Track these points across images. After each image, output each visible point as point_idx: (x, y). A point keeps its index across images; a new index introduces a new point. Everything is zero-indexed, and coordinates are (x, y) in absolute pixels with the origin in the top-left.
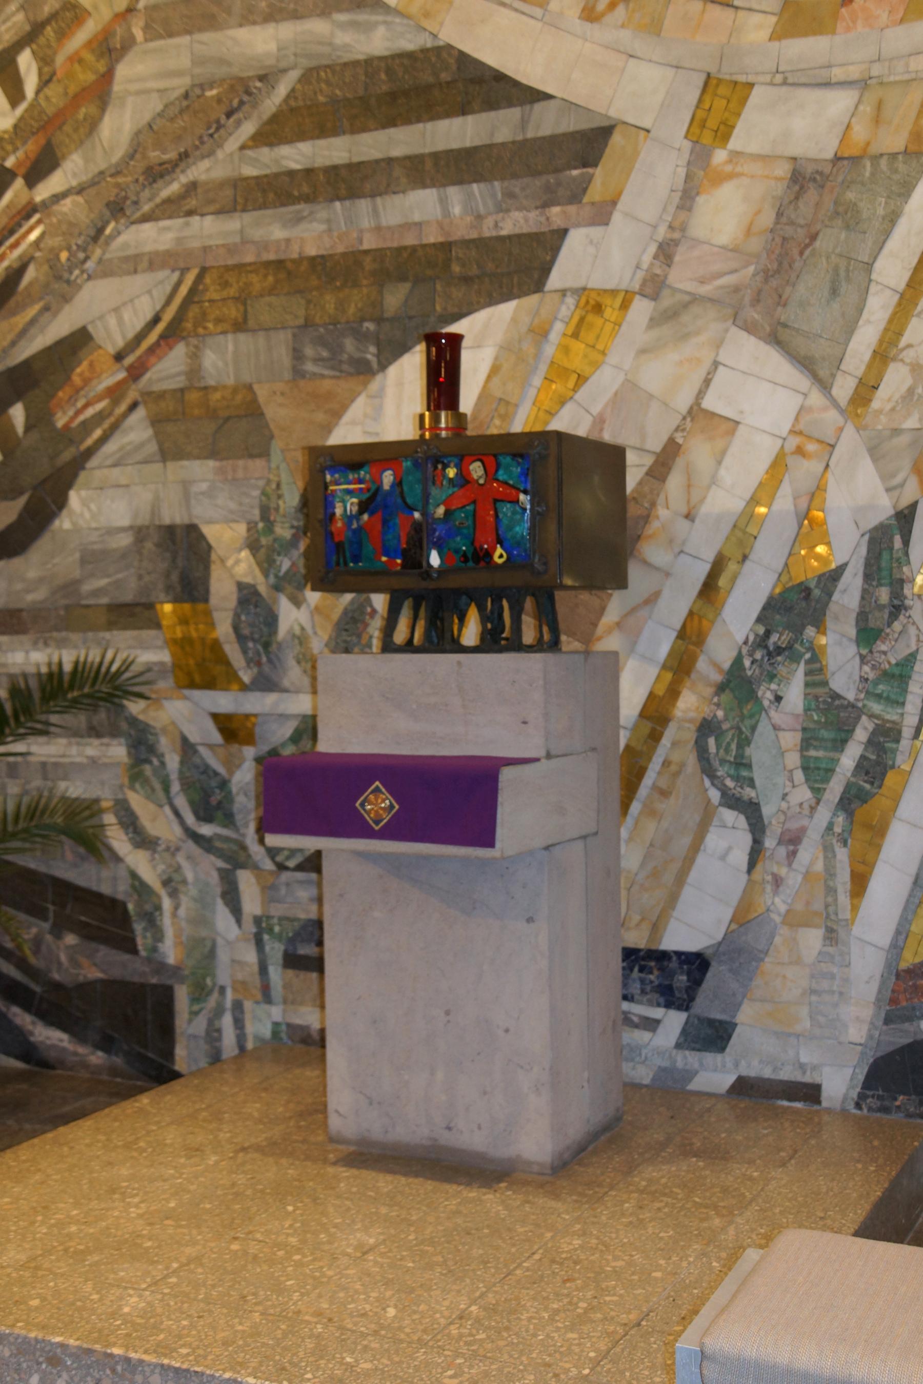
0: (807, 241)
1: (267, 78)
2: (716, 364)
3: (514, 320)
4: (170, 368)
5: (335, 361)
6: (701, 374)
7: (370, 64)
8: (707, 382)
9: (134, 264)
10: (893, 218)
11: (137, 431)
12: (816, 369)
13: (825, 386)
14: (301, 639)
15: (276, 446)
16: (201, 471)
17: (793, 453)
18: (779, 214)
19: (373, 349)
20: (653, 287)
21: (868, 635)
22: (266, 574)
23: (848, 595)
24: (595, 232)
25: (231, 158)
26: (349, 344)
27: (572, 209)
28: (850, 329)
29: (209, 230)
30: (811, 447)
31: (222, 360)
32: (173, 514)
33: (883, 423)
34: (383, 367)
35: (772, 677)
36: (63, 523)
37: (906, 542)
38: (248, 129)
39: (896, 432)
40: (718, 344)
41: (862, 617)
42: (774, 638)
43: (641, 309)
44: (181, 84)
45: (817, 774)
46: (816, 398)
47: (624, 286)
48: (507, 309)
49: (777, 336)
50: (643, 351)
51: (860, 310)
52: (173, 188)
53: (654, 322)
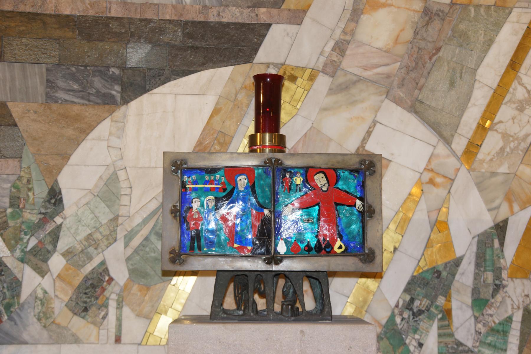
0: (434, 51)
2: (375, 123)
3: (231, 79)
5: (85, 94)
6: (365, 127)
8: (369, 133)
10: (489, 43)
12: (443, 132)
13: (448, 142)
14: (44, 301)
15: (28, 153)
17: (427, 183)
18: (416, 33)
19: (117, 88)
20: (332, 68)
21: (480, 303)
22: (12, 248)
23: (466, 276)
24: (292, 29)
26: (98, 83)
27: (274, 11)
28: (463, 108)
30: (439, 180)
33: (485, 168)
34: (126, 101)
35: (416, 331)
37: (502, 244)
39: (494, 174)
40: (377, 110)
41: (475, 291)
42: (417, 303)
43: (323, 82)
46: (442, 149)
47: (312, 65)
48: (226, 71)
49: (416, 108)
50: (325, 109)
51: (469, 96)
53: (332, 91)
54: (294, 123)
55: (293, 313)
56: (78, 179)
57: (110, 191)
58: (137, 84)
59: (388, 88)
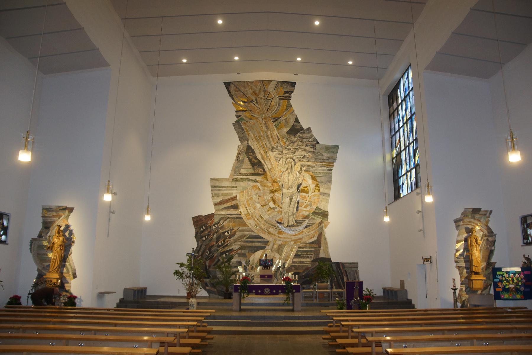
4: (239, 251)
11: (237, 255)
16: (242, 258)
25: (244, 239)
29: (243, 243)
31: (243, 251)
32: (239, 261)
56: (251, 259)
57: (253, 260)
58: (256, 251)
59: (276, 251)
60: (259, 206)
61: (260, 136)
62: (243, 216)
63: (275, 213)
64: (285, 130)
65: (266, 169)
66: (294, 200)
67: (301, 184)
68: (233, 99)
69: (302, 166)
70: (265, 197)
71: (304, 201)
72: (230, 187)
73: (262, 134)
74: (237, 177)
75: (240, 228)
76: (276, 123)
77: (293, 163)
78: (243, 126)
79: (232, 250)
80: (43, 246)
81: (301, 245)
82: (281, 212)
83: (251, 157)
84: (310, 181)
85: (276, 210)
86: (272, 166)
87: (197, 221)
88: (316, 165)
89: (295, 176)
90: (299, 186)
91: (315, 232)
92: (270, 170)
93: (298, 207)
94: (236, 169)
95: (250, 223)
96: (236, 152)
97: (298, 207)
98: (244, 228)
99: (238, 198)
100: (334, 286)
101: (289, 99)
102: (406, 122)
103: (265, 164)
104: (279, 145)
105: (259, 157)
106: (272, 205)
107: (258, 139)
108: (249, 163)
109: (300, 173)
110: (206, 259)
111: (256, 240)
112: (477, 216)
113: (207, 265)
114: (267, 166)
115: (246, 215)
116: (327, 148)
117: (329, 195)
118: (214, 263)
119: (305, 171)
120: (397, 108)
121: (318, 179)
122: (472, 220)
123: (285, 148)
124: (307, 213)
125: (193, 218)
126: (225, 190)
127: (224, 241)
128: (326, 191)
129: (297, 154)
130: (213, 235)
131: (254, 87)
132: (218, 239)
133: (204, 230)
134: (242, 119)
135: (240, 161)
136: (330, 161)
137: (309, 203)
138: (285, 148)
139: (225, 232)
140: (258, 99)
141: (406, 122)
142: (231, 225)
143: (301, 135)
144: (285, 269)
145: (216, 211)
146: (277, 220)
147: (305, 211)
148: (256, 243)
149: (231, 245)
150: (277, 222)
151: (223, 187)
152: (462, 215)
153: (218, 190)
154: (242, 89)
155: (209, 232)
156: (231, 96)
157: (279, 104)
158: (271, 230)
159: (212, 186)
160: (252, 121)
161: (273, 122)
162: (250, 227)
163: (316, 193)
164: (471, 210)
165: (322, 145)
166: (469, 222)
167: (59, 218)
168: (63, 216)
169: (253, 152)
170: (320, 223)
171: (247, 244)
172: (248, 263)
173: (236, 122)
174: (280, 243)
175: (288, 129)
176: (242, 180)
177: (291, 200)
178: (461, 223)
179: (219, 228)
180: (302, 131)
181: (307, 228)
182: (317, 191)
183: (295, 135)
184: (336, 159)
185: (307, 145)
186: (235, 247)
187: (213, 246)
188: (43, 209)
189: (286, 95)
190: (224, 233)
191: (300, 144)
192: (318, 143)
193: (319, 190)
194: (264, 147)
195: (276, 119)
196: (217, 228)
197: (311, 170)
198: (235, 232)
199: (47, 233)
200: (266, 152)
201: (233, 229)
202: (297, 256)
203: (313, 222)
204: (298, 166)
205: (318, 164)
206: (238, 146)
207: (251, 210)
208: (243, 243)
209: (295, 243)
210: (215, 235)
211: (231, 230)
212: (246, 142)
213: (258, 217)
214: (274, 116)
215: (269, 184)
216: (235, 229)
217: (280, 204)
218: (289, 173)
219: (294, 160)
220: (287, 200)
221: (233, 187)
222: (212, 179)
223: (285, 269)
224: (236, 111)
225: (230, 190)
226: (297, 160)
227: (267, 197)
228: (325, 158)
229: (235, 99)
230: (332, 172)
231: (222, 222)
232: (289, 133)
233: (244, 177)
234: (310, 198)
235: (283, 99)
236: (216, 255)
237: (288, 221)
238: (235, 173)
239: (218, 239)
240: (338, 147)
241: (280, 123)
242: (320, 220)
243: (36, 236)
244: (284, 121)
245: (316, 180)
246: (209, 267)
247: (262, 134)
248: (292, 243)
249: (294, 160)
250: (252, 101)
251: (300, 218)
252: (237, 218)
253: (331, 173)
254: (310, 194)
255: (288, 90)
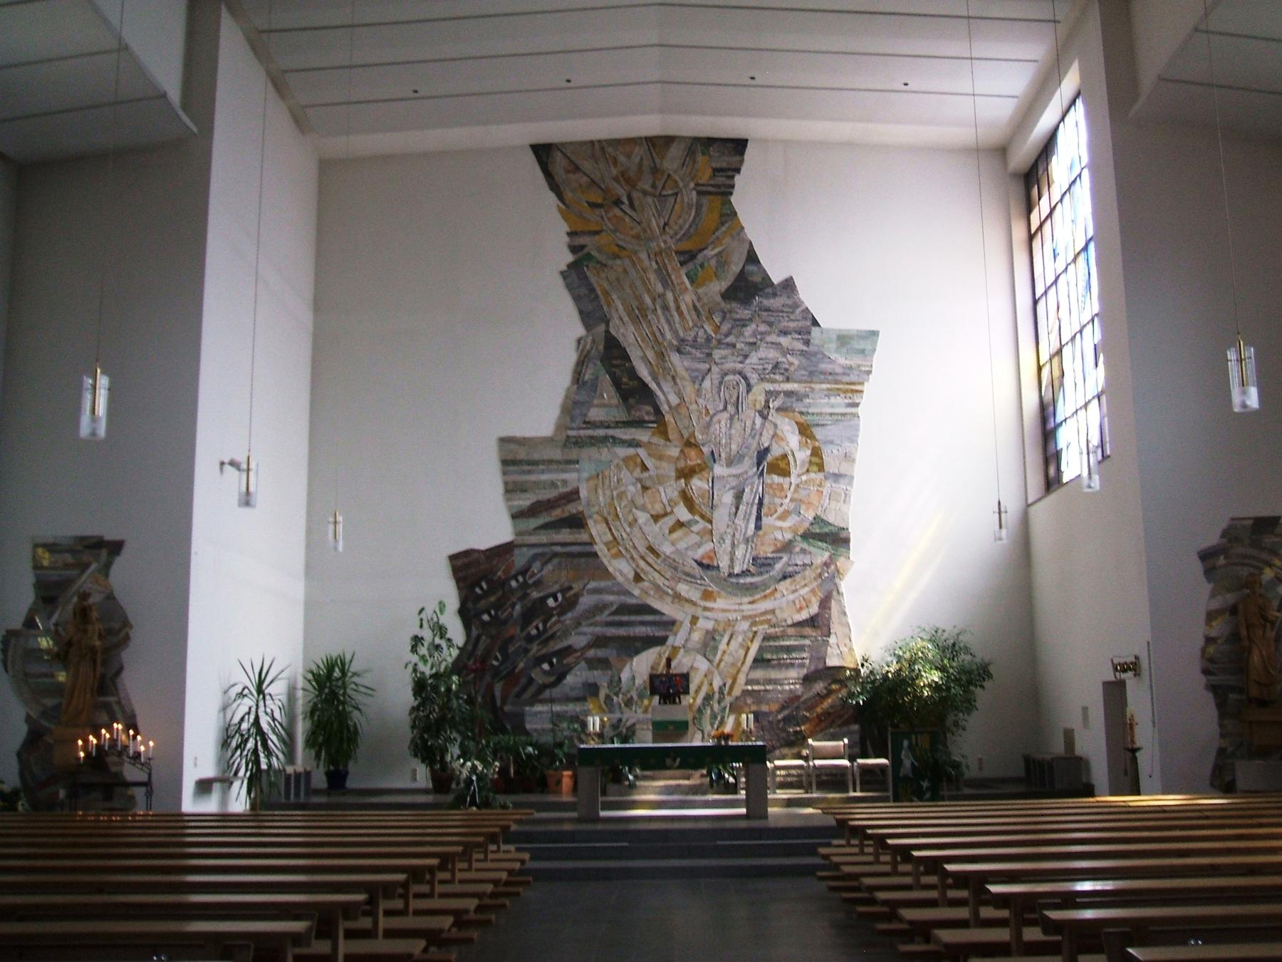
1: (612, 604)
4: (591, 653)
7: (632, 605)
9: (585, 634)
11: (583, 664)
23: (717, 696)
25: (604, 617)
31: (600, 653)
32: (591, 681)
36: (565, 682)
38: (607, 612)
44: (593, 603)
45: (712, 725)
49: (705, 656)
52: (591, 621)
54: (673, 664)
55: (674, 702)
56: (625, 676)
59: (698, 651)
60: (643, 517)
61: (643, 309)
62: (600, 548)
63: (695, 538)
64: (716, 287)
65: (665, 408)
66: (746, 497)
67: (767, 450)
68: (560, 196)
69: (769, 394)
70: (661, 490)
71: (777, 501)
72: (558, 462)
73: (648, 300)
74: (578, 432)
75: (592, 585)
76: (691, 265)
77: (743, 387)
78: (593, 279)
79: (569, 650)
80: (41, 650)
81: (772, 630)
82: (711, 531)
83: (618, 372)
84: (793, 440)
85: (695, 528)
86: (682, 398)
87: (467, 566)
88: (812, 390)
89: (749, 424)
90: (763, 454)
91: (813, 591)
92: (674, 409)
93: (759, 518)
94: (573, 408)
95: (621, 568)
96: (572, 357)
97: (759, 518)
98: (603, 584)
99: (583, 493)
100: (869, 748)
101: (727, 191)
102: (1074, 260)
103: (659, 393)
104: (701, 333)
105: (644, 373)
106: (683, 513)
107: (639, 315)
108: (612, 390)
109: (765, 417)
110: (493, 678)
111: (639, 618)
112: (1269, 540)
113: (498, 693)
114: (667, 396)
115: (606, 544)
116: (844, 340)
117: (852, 477)
118: (516, 690)
119: (778, 410)
120: (1050, 215)
121: (819, 433)
122: (1254, 552)
123: (719, 342)
124: (788, 536)
125: (453, 558)
126: (543, 472)
127: (545, 625)
128: (844, 469)
129: (753, 359)
130: (513, 606)
131: (622, 158)
132: (527, 618)
133: (486, 594)
134: (589, 257)
135: (584, 383)
136: (853, 378)
137: (792, 506)
138: (719, 342)
139: (547, 597)
140: (635, 195)
141: (1074, 260)
142: (564, 577)
143: (766, 303)
144: (728, 700)
145: (518, 534)
146: (697, 557)
147: (780, 528)
148: (639, 626)
149: (566, 633)
150: (700, 564)
151: (535, 463)
152: (1223, 536)
153: (524, 472)
154: (587, 165)
155: (499, 599)
156: (555, 187)
157: (699, 207)
158: (683, 588)
159: (505, 462)
160: (618, 262)
161: (682, 264)
162: (620, 579)
163: (812, 475)
164: (1251, 522)
165: (828, 330)
166: (1245, 557)
167: (83, 572)
168: (94, 566)
169: (627, 358)
170: (826, 565)
171: (612, 631)
172: (615, 684)
173: (570, 266)
174: (710, 625)
175: (724, 285)
176: (594, 441)
177: (739, 497)
178: (1222, 560)
179: (529, 586)
180: (769, 290)
181: (788, 581)
182: (815, 468)
183: (746, 302)
184: (869, 372)
185: (785, 333)
186: (578, 641)
187: (512, 638)
188: (36, 546)
189: (720, 180)
190: (543, 600)
191: (763, 328)
192: (815, 323)
193: (821, 467)
194: (656, 341)
195: (688, 257)
196: (524, 586)
197: (799, 407)
198: (577, 596)
199: (50, 616)
200: (661, 356)
201: (570, 588)
202: (759, 662)
203: (807, 561)
204: (758, 394)
205: (817, 387)
206: (579, 341)
207: (622, 532)
208: (598, 630)
209: (754, 624)
210: (518, 607)
211: (564, 590)
212: (602, 327)
213: (642, 549)
214: (686, 246)
215: (674, 452)
216: (576, 587)
217: (706, 510)
218: (731, 418)
219: (745, 378)
220: (728, 498)
221: (569, 462)
222: (504, 441)
223: (728, 700)
224: (569, 234)
225: (557, 471)
226: (754, 378)
227: (669, 491)
228: (839, 370)
229: (569, 195)
230: (860, 410)
231: (536, 567)
232: (728, 295)
233: (601, 432)
234: (795, 491)
235: (709, 193)
236: (521, 665)
237: (732, 560)
238: (572, 420)
239: (527, 618)
240: (874, 334)
241: (702, 266)
242: (827, 555)
243: (17, 624)
244: (713, 262)
245: (812, 437)
246: (504, 700)
247: (648, 300)
248: (745, 625)
249: (745, 378)
250: (618, 202)
251: (766, 550)
252: (580, 555)
253: (856, 416)
254: (793, 479)
255: (724, 165)
